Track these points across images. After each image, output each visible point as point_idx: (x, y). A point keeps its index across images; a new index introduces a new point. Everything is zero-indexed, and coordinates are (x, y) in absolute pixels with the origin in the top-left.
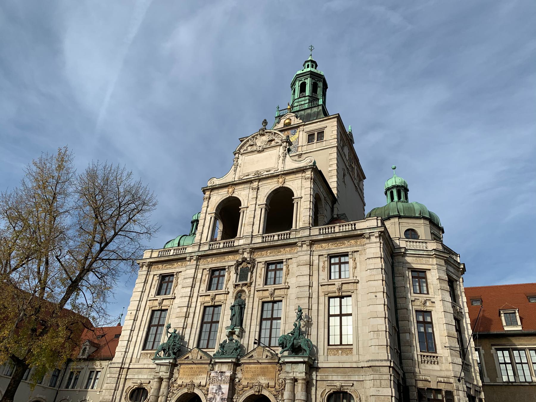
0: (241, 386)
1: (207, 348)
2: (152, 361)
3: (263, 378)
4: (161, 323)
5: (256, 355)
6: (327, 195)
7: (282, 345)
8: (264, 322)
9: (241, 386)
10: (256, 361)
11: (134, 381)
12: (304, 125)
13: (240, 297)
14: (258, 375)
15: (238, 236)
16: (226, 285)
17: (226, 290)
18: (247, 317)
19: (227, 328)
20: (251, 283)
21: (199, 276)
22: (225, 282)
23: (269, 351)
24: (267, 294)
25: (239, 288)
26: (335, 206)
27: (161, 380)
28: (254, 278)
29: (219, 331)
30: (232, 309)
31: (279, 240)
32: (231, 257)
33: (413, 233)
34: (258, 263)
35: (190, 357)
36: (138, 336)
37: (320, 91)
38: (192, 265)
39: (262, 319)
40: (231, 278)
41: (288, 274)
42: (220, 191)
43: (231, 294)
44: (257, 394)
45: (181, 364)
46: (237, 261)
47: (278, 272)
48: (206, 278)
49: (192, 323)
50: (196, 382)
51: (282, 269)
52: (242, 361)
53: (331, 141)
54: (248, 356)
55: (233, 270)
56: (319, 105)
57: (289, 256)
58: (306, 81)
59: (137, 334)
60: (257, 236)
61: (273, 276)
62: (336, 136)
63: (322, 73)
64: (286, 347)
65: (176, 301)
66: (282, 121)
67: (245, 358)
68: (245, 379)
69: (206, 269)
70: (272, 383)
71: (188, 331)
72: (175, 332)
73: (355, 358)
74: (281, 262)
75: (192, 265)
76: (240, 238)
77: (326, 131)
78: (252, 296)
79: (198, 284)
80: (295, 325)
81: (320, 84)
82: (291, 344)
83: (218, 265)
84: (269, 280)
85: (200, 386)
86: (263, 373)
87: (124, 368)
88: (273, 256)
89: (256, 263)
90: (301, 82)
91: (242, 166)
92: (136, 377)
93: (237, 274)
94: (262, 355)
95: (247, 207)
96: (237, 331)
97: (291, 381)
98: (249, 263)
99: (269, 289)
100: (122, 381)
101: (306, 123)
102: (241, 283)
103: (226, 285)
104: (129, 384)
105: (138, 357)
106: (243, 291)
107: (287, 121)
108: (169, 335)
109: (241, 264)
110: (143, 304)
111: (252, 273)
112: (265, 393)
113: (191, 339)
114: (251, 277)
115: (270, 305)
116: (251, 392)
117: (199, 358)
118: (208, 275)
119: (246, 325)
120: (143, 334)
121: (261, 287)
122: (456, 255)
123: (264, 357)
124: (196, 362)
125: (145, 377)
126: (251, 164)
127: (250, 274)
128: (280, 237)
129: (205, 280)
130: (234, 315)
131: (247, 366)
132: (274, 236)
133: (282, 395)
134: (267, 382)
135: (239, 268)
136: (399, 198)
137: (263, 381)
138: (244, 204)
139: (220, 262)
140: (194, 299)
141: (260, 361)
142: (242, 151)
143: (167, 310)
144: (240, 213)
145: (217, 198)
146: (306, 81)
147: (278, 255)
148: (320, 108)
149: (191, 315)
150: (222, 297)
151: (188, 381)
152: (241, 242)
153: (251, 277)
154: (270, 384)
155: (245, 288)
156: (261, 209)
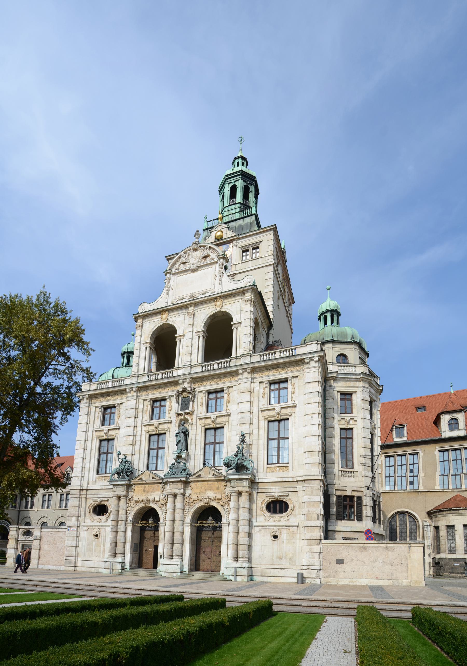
0: (192, 499)
1: (156, 470)
2: (108, 483)
3: (211, 492)
4: (109, 451)
5: (203, 474)
6: (264, 319)
7: (228, 465)
8: (207, 447)
9: (192, 499)
10: (204, 479)
11: (95, 499)
12: (238, 239)
13: (183, 425)
15: (176, 366)
16: (169, 414)
17: (169, 419)
18: (191, 442)
19: (174, 453)
20: (193, 412)
21: (141, 407)
22: (167, 412)
23: (214, 471)
24: (209, 421)
26: (271, 332)
27: (119, 498)
28: (195, 407)
29: (165, 456)
30: (177, 436)
31: (219, 369)
33: (344, 358)
34: (199, 392)
35: (144, 479)
36: (90, 463)
37: (251, 196)
38: (133, 396)
39: (205, 444)
40: (172, 408)
41: (229, 402)
42: (152, 318)
43: (174, 423)
44: (206, 505)
45: (135, 484)
46: (178, 391)
47: (218, 400)
48: (149, 408)
49: (140, 450)
50: (151, 498)
51: (223, 397)
52: (191, 480)
53: (267, 258)
54: (196, 475)
55: (174, 400)
56: (251, 215)
58: (236, 183)
59: (89, 461)
60: (196, 366)
61: (214, 404)
62: (272, 253)
63: (254, 174)
64: (231, 466)
65: (122, 431)
66: (213, 234)
67: (194, 477)
68: (195, 493)
69: (146, 400)
70: (219, 496)
71: (136, 456)
72: (125, 458)
74: (222, 391)
75: (133, 396)
76: (179, 368)
77: (261, 245)
78: (194, 423)
79: (140, 415)
81: (252, 188)
82: (235, 464)
84: (210, 408)
85: (154, 501)
86: (211, 489)
87: (83, 490)
88: (214, 385)
89: (197, 393)
90: (231, 185)
91: (174, 288)
92: (95, 496)
93: (179, 404)
94: (207, 474)
95: (183, 335)
96: (184, 455)
97: (236, 494)
98: (190, 393)
99: (211, 416)
100: (84, 500)
101: (240, 236)
102: (183, 412)
103: (169, 414)
105: (94, 480)
106: (186, 421)
107: (219, 233)
108: (120, 460)
109: (181, 394)
110: (90, 434)
111: (193, 402)
112: (214, 504)
113: (139, 464)
114: (193, 406)
115: (213, 431)
116: (201, 504)
117: (151, 479)
118: (149, 406)
119: (191, 449)
120: (94, 461)
121: (204, 414)
122: (377, 377)
123: (211, 475)
124: (149, 482)
125: (104, 496)
126: (184, 286)
127: (191, 403)
128: (220, 365)
129: (147, 411)
130: (179, 441)
131: (196, 483)
132: (213, 365)
133: (229, 504)
134: (214, 495)
135: (180, 399)
136: (332, 322)
137: (211, 495)
138: (180, 332)
139: (160, 393)
140: (139, 429)
141: (207, 479)
142: (174, 271)
143: (114, 439)
144: (176, 342)
145: (151, 326)
146: (236, 183)
148: (254, 218)
149: (138, 443)
150: (166, 426)
151: (144, 498)
152: (180, 372)
153: (193, 406)
154: (217, 497)
155: (187, 417)
156: (199, 337)
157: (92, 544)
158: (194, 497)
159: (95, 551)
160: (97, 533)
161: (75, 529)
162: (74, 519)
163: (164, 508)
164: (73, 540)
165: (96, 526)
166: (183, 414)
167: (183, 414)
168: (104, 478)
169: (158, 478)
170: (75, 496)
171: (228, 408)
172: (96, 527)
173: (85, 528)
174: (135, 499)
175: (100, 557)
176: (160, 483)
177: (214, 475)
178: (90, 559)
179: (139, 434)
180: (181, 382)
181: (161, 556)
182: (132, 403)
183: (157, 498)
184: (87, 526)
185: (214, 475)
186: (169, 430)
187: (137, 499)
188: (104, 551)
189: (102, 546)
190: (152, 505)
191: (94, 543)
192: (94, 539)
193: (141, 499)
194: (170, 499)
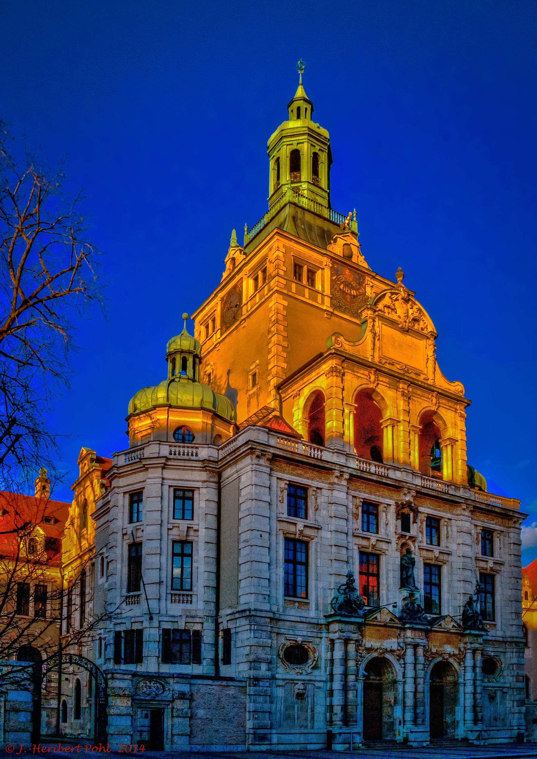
3: (449, 646)
14: (445, 643)
16: (386, 530)
25: (404, 541)
32: (386, 492)
57: (449, 516)
65: (325, 534)
67: (435, 626)
68: (434, 646)
70: (457, 652)
73: (500, 633)
80: (471, 599)
83: (373, 498)
92: (291, 632)
104: (282, 640)
123: (450, 626)
137: (449, 649)
139: (375, 495)
147: (439, 511)
150: (384, 546)
155: (410, 542)
157: (294, 707)
158: (434, 650)
159: (298, 719)
160: (304, 691)
161: (268, 684)
162: (264, 666)
163: (402, 661)
164: (266, 702)
165: (298, 680)
166: (407, 538)
167: (407, 538)
168: (297, 604)
169: (397, 621)
170: (264, 628)
171: (448, 545)
172: (300, 683)
173: (281, 683)
174: (367, 646)
175: (306, 727)
176: (397, 628)
177: (454, 626)
178: (293, 731)
179: (350, 546)
180: (405, 491)
181: (400, 722)
182: (340, 495)
183: (395, 647)
184: (284, 680)
185: (454, 626)
186: (386, 552)
187: (370, 646)
188: (313, 718)
189: (309, 711)
190: (387, 656)
191: (296, 706)
192: (295, 700)
193: (376, 648)
194: (410, 652)
